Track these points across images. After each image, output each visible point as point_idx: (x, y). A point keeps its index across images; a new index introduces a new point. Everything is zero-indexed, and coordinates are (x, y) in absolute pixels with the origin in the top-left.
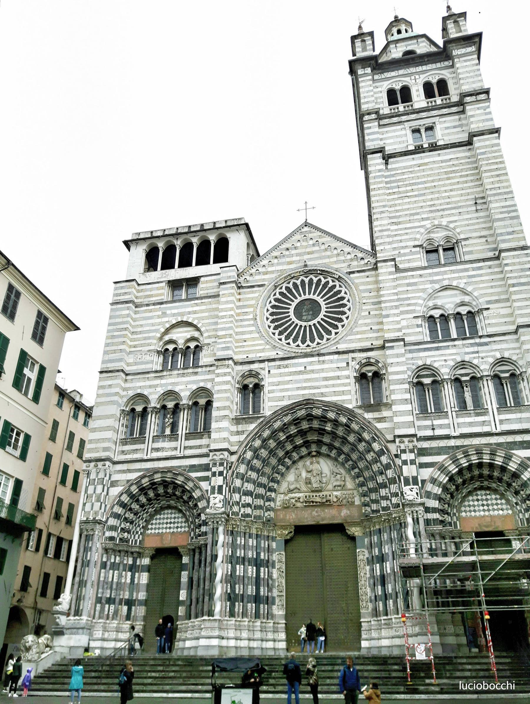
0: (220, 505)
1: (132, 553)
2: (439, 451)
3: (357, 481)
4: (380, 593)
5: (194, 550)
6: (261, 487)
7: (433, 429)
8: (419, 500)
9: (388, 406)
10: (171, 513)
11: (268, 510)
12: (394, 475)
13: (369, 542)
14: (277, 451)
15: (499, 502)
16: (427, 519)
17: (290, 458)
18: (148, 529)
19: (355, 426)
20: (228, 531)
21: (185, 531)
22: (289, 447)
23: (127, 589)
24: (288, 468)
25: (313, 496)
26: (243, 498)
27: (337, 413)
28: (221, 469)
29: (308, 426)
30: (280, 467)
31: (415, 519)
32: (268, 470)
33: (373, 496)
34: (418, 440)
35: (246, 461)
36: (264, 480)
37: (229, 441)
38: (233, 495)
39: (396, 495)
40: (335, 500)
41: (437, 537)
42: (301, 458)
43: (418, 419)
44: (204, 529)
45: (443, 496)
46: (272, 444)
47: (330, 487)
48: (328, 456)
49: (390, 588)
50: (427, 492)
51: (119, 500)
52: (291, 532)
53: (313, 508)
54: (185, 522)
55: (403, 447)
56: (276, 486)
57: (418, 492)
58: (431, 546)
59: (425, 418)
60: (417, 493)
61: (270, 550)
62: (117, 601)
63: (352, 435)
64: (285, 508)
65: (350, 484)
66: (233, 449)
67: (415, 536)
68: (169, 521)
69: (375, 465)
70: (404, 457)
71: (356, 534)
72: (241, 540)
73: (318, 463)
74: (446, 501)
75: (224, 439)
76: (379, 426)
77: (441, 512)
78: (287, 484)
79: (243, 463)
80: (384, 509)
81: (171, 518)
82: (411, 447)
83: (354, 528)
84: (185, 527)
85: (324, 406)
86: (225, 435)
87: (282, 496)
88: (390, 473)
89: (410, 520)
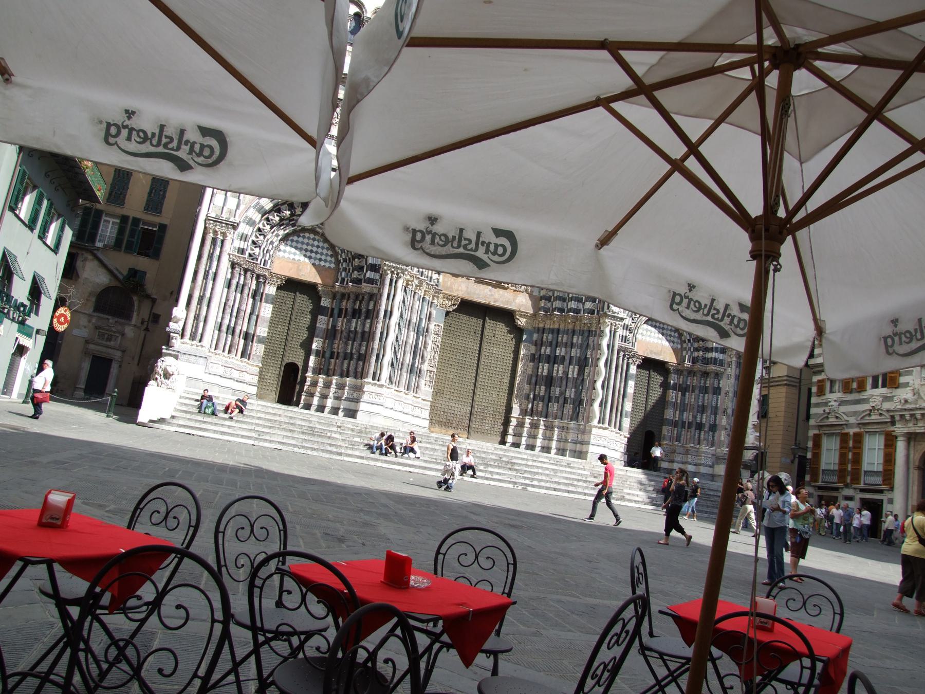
1: (258, 277)
4: (542, 393)
5: (343, 295)
10: (314, 239)
15: (673, 334)
18: (280, 250)
21: (329, 267)
23: (246, 320)
44: (370, 274)
49: (556, 391)
51: (258, 203)
54: (331, 256)
62: (238, 331)
68: (310, 248)
81: (313, 246)
84: (330, 262)
89: (607, 330)
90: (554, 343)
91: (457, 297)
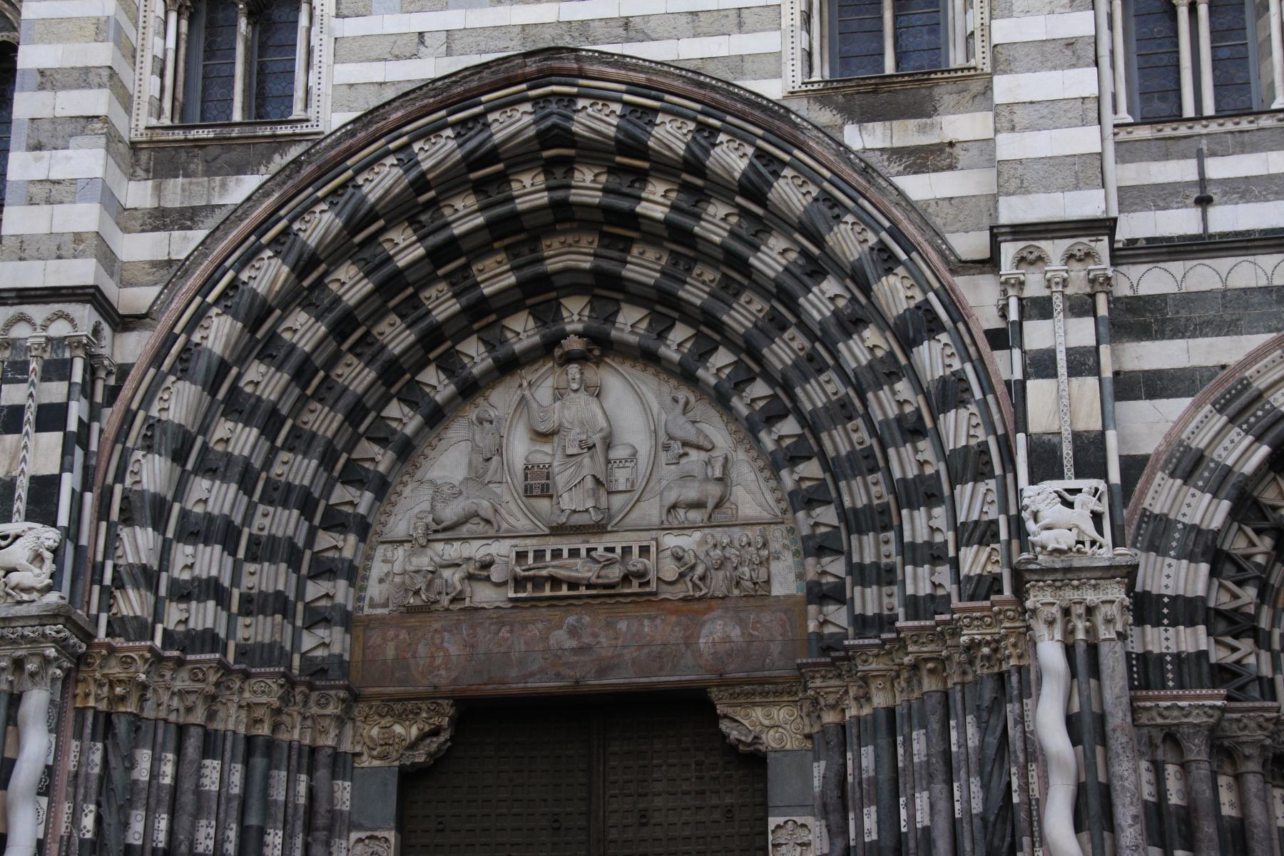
0: (37, 576)
2: (1226, 312)
3: (788, 479)
6: (285, 505)
7: (1204, 202)
8: (1106, 554)
9: (975, 87)
11: (316, 618)
12: (981, 434)
13: (833, 780)
14: (383, 327)
16: (1145, 657)
17: (449, 365)
19: (790, 193)
20: (80, 712)
22: (442, 304)
24: (436, 417)
25: (557, 554)
26: (183, 553)
27: (702, 127)
28: (55, 392)
29: (543, 198)
30: (394, 410)
31: (1081, 650)
32: (324, 421)
33: (868, 549)
34: (1117, 257)
35: (201, 366)
36: (299, 469)
37: (107, 258)
38: (125, 533)
39: (984, 533)
40: (670, 570)
41: (1197, 750)
42: (508, 366)
43: (1126, 152)
45: (1238, 545)
46: (351, 284)
47: (651, 511)
48: (647, 357)
50: (1147, 517)
52: (435, 732)
53: (556, 613)
55: (1035, 287)
56: (365, 500)
57: (1103, 508)
58: (1161, 792)
59: (1165, 150)
60: (1097, 517)
61: (321, 821)
63: (776, 243)
64: (412, 610)
65: (752, 496)
66: (138, 298)
67: (1075, 739)
69: (884, 394)
70: (1038, 335)
71: (770, 740)
72: (156, 761)
73: (597, 393)
74: (1253, 572)
75: (78, 237)
76: (918, 187)
77: (1222, 626)
78: (426, 493)
79: (183, 369)
80: (915, 606)
82: (1078, 286)
83: (758, 713)
85: (634, 88)
86: (84, 216)
87: (400, 552)
88: (959, 428)
89: (1051, 653)
90: (884, 776)
91: (433, 696)
